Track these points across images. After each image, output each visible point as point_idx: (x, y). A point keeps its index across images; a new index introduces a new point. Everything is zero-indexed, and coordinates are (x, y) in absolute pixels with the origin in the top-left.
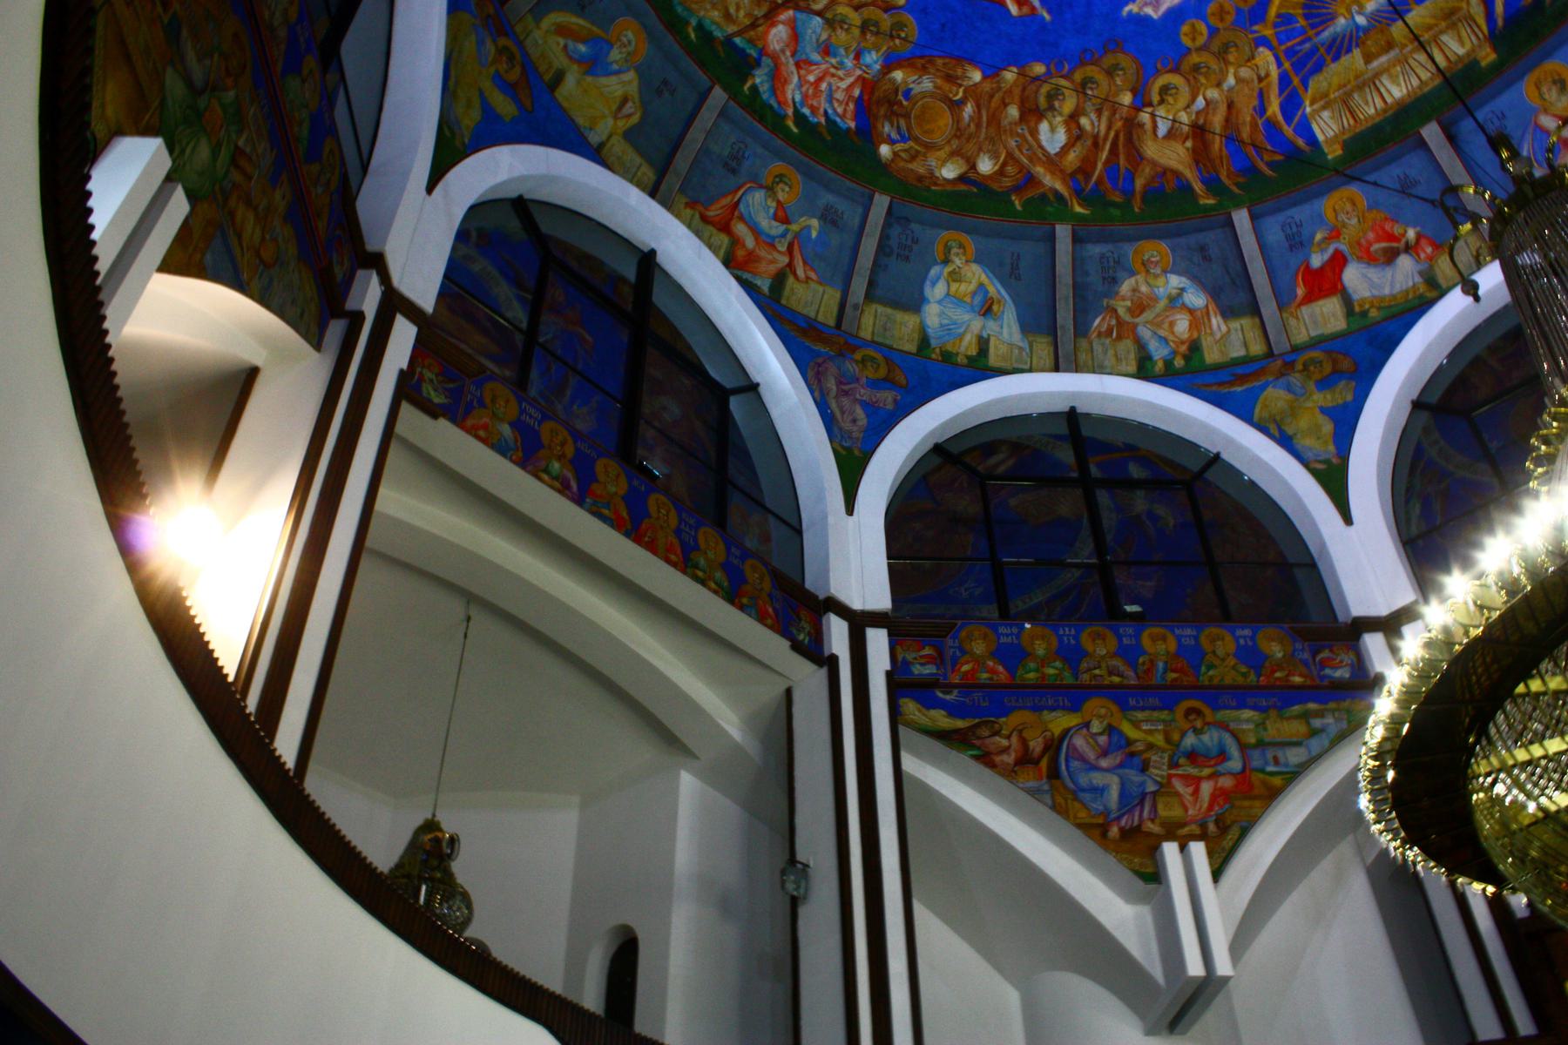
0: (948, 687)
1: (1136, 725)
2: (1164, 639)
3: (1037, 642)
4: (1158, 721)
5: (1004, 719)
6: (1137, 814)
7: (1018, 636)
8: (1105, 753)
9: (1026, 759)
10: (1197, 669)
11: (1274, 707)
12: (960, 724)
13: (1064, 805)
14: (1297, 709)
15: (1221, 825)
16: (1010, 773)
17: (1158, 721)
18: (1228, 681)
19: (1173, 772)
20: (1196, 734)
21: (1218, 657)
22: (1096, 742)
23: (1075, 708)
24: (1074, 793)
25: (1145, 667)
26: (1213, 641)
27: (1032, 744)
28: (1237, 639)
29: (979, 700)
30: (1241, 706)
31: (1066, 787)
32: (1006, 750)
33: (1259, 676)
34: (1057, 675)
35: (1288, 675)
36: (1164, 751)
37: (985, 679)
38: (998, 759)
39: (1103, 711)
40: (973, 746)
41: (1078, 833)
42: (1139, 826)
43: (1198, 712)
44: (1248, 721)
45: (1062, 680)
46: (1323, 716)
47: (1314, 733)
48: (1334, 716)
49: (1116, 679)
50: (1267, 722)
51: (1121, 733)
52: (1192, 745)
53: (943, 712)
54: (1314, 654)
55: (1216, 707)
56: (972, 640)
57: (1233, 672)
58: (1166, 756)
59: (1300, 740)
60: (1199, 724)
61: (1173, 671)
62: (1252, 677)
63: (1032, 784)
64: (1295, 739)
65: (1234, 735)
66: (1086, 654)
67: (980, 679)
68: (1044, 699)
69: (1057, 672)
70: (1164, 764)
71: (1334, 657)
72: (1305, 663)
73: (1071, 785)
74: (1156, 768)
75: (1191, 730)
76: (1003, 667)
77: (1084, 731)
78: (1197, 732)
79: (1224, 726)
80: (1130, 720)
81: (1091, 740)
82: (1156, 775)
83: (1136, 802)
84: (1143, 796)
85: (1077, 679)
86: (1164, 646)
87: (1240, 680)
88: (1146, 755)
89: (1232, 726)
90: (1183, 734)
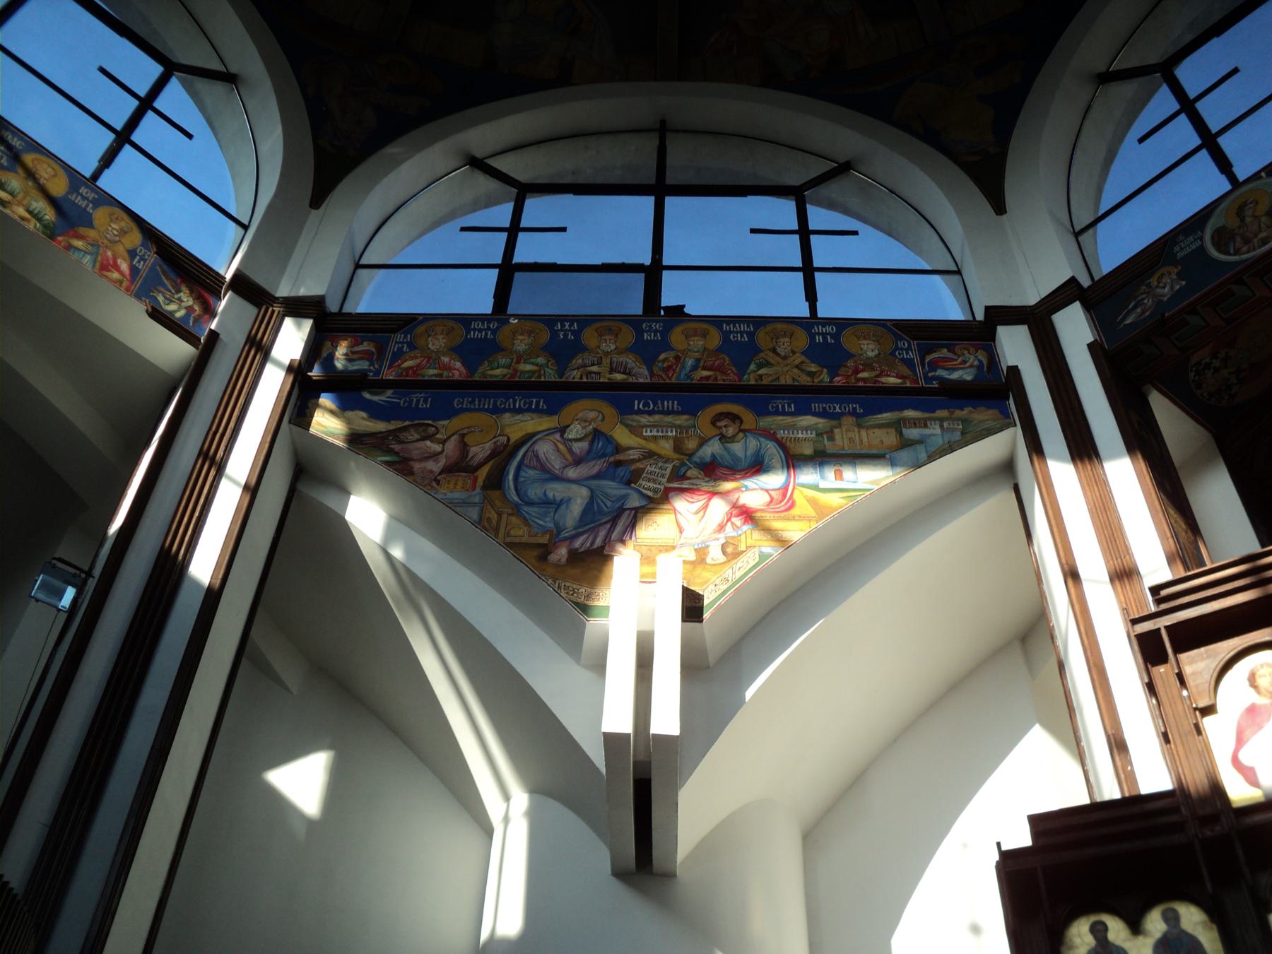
0: (383, 385)
1: (635, 430)
2: (704, 335)
3: (520, 337)
4: (673, 426)
5: (445, 422)
6: (602, 533)
7: (494, 332)
8: (578, 461)
9: (460, 466)
10: (742, 368)
11: (854, 414)
12: (380, 426)
13: (494, 522)
14: (887, 416)
15: (729, 550)
16: (429, 483)
17: (673, 426)
18: (786, 380)
19: (675, 485)
20: (722, 443)
21: (778, 354)
22: (570, 450)
23: (552, 410)
24: (517, 505)
25: (665, 365)
26: (776, 336)
27: (473, 450)
28: (812, 336)
29: (418, 401)
30: (803, 410)
31: (504, 496)
32: (434, 456)
33: (832, 376)
34: (534, 372)
35: (877, 376)
36: (668, 460)
37: (431, 376)
38: (417, 466)
39: (592, 415)
40: (391, 452)
41: (507, 554)
42: (602, 548)
43: (734, 418)
44: (806, 429)
45: (539, 376)
46: (926, 426)
47: (906, 444)
48: (942, 427)
49: (619, 377)
50: (836, 431)
51: (609, 440)
52: (713, 455)
53: (364, 414)
54: (924, 352)
55: (761, 411)
56: (429, 336)
57: (796, 371)
58: (670, 467)
59: (882, 452)
60: (730, 431)
61: (704, 368)
62: (825, 377)
63: (458, 495)
64: (874, 451)
65: (782, 445)
66: (584, 349)
67: (423, 376)
68: (511, 400)
69: (535, 368)
70: (663, 476)
71: (955, 357)
72: (909, 363)
73: (516, 498)
74: (649, 480)
75: (718, 438)
76: (462, 363)
77: (557, 436)
78: (723, 439)
79: (772, 436)
80: (626, 426)
81: (561, 447)
82: (646, 489)
83: (607, 519)
84: (621, 511)
85: (561, 375)
86: (701, 343)
87: (805, 380)
88: (639, 465)
89: (781, 434)
90: (703, 442)
